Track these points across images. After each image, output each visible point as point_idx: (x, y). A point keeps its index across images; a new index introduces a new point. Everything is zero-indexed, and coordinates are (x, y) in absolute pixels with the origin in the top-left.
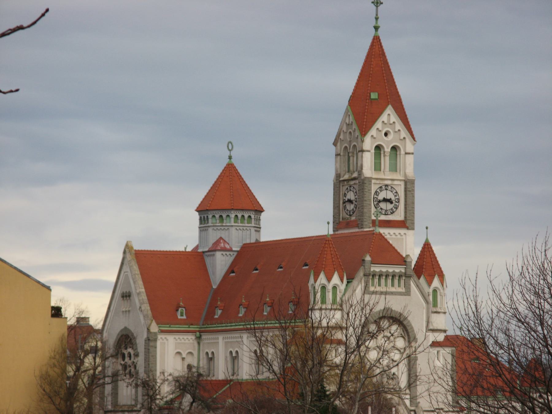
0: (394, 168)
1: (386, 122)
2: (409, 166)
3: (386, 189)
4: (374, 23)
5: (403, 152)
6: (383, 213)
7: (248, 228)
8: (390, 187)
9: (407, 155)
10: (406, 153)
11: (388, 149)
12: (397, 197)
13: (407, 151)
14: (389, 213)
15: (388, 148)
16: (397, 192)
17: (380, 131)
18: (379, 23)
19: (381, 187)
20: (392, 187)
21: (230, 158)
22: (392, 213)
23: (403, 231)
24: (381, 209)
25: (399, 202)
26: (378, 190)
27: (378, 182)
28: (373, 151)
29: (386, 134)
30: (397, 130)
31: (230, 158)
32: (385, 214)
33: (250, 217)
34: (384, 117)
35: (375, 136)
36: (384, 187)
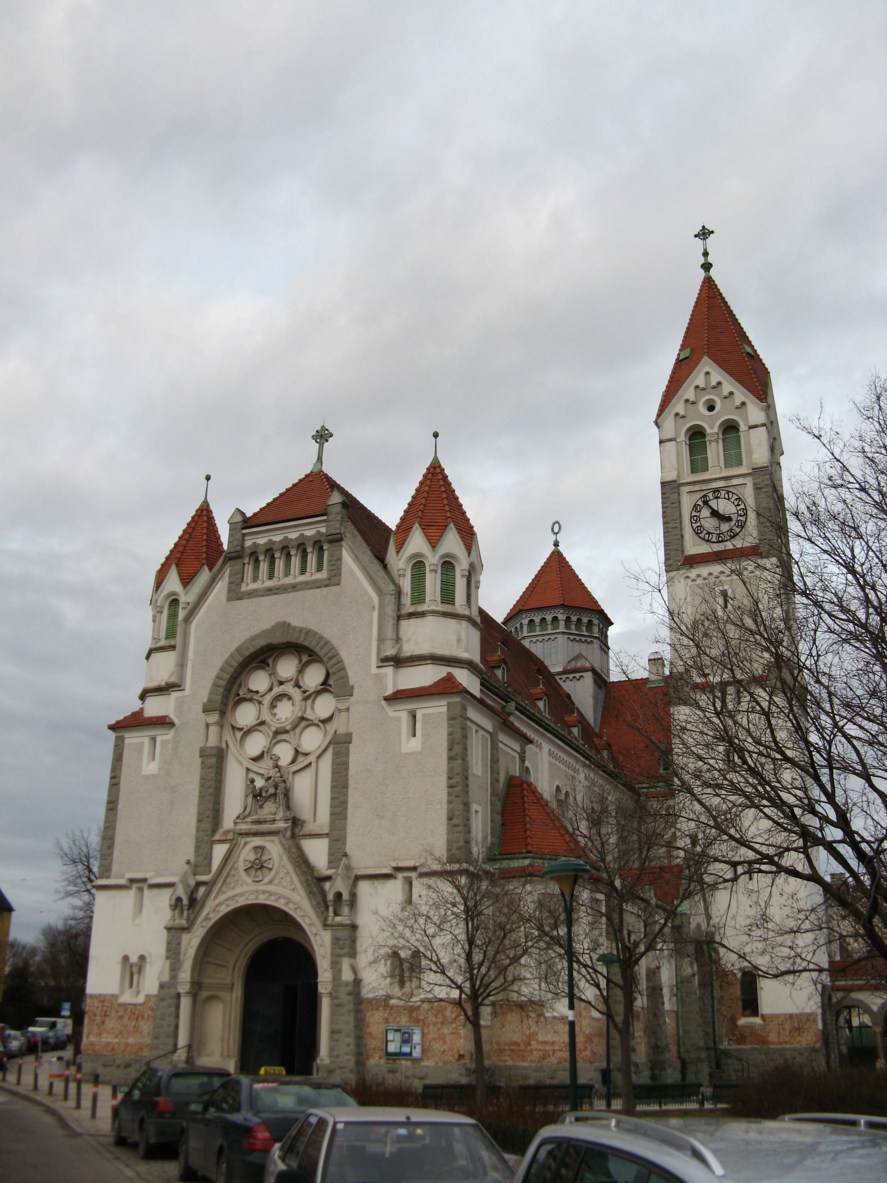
0: (733, 457)
4: (702, 260)
5: (743, 427)
7: (553, 637)
8: (723, 493)
9: (751, 430)
10: (751, 427)
11: (712, 430)
12: (742, 506)
13: (752, 423)
15: (712, 427)
16: (739, 499)
17: (693, 403)
18: (710, 259)
19: (705, 496)
20: (728, 492)
21: (556, 544)
24: (709, 533)
25: (746, 514)
27: (697, 488)
28: (682, 438)
29: (711, 408)
31: (556, 544)
32: (719, 542)
33: (555, 619)
35: (682, 413)
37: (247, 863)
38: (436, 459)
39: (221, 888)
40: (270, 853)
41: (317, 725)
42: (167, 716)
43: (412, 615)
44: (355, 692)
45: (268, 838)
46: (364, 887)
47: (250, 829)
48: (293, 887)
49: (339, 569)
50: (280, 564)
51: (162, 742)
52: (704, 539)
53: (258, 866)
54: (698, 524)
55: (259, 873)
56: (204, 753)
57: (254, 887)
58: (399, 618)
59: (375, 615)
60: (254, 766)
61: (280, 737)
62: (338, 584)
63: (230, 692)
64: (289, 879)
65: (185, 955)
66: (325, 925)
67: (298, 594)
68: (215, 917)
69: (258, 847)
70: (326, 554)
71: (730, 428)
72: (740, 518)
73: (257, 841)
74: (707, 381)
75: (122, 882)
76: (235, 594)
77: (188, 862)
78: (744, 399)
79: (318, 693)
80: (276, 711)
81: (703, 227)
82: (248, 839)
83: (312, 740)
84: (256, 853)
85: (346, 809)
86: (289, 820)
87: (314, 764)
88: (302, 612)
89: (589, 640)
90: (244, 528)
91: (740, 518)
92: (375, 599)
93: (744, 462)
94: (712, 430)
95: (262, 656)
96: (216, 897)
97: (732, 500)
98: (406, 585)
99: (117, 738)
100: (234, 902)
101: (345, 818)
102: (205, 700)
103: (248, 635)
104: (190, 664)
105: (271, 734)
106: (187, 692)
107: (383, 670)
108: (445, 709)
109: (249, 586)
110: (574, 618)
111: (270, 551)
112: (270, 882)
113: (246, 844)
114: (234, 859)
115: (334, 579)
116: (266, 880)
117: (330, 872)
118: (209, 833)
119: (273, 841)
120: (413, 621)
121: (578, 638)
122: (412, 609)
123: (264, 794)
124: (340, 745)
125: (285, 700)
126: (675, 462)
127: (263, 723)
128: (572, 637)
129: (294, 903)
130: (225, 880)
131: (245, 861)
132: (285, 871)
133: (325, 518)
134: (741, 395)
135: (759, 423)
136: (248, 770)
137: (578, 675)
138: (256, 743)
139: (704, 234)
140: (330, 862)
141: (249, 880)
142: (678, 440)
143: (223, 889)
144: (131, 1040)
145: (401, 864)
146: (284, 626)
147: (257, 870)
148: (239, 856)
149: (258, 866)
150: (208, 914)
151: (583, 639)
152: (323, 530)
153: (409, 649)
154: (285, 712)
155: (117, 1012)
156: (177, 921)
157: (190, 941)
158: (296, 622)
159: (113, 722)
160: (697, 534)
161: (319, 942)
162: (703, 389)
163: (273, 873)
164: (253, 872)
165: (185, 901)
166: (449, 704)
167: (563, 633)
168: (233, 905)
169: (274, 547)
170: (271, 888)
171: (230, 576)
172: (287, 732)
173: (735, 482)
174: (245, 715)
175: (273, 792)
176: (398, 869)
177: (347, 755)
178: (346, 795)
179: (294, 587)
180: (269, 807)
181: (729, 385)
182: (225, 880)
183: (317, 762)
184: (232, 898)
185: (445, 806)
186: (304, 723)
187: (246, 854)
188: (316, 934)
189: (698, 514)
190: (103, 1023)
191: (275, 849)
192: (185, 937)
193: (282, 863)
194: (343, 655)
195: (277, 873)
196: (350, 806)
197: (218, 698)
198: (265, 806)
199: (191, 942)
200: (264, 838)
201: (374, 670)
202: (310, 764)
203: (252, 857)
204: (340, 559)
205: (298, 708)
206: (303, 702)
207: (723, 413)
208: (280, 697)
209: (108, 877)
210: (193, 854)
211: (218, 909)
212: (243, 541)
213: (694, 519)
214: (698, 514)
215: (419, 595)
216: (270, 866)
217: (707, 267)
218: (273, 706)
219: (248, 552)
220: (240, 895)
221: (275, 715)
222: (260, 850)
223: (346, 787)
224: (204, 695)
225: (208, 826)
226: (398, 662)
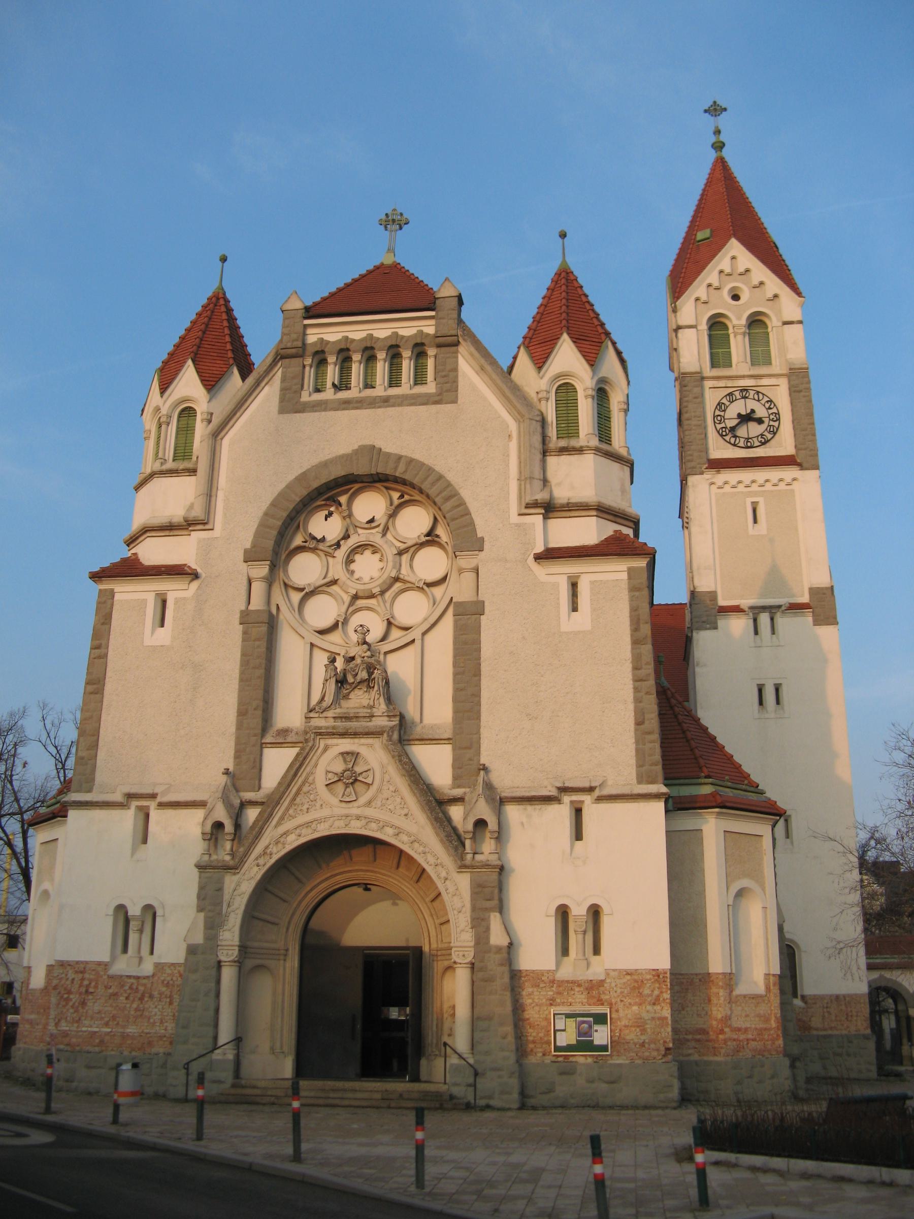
1: (728, 270)
2: (790, 345)
3: (745, 398)
4: (713, 139)
5: (773, 323)
8: (752, 393)
10: (785, 323)
12: (775, 410)
14: (757, 444)
15: (739, 318)
16: (771, 401)
17: (717, 289)
18: (722, 138)
20: (758, 393)
22: (763, 444)
23: (789, 473)
25: (778, 420)
26: (724, 401)
27: (722, 383)
28: (704, 326)
29: (736, 297)
30: (756, 283)
34: (722, 261)
35: (704, 298)
36: (737, 393)
37: (330, 775)
39: (287, 809)
40: (366, 762)
41: (421, 589)
42: (185, 565)
43: (563, 451)
44: (487, 546)
45: (363, 741)
46: (512, 812)
47: (334, 728)
48: (406, 811)
49: (455, 381)
51: (177, 601)
52: (730, 443)
53: (350, 779)
55: (350, 789)
56: (246, 618)
57: (343, 810)
58: (545, 453)
59: (513, 445)
60: (317, 640)
61: (360, 603)
62: (455, 401)
63: (281, 539)
64: (398, 800)
65: (229, 906)
66: (463, 867)
68: (278, 853)
69: (348, 753)
70: (430, 363)
71: (756, 322)
72: (772, 423)
73: (346, 745)
74: (733, 267)
75: (118, 797)
76: (290, 403)
77: (227, 772)
79: (422, 545)
80: (353, 566)
81: (715, 102)
82: (330, 742)
83: (411, 608)
84: (345, 761)
85: (479, 704)
86: (394, 716)
87: (418, 642)
90: (305, 318)
91: (772, 423)
92: (513, 426)
94: (737, 320)
95: (331, 489)
96: (279, 824)
97: (763, 402)
100: (309, 831)
101: (478, 718)
102: (248, 545)
103: (315, 460)
104: (221, 495)
105: (347, 599)
106: (217, 532)
108: (625, 576)
111: (344, 354)
112: (369, 803)
113: (326, 748)
114: (308, 769)
115: (448, 392)
116: (363, 800)
117: (458, 792)
118: (259, 731)
119: (371, 746)
120: (565, 459)
122: (563, 443)
123: (350, 679)
124: (468, 617)
125: (368, 553)
126: (696, 353)
127: (334, 582)
129: (409, 835)
130: (294, 799)
131: (328, 772)
132: (392, 789)
133: (432, 313)
135: (795, 319)
136: (312, 645)
138: (322, 611)
139: (715, 110)
140: (456, 778)
141: (334, 801)
142: (699, 328)
143: (291, 812)
144: (131, 1030)
146: (372, 451)
147: (347, 786)
148: (316, 766)
149: (350, 779)
150: (267, 847)
152: (431, 330)
153: (562, 494)
154: (368, 568)
155: (107, 987)
156: (214, 857)
157: (238, 884)
158: (389, 447)
159: (97, 569)
161: (451, 889)
162: (729, 275)
163: (373, 789)
164: (340, 787)
165: (229, 827)
166: (630, 571)
168: (308, 835)
169: (352, 347)
170: (369, 812)
171: (283, 380)
172: (372, 596)
173: (765, 382)
174: (305, 569)
175: (359, 674)
176: (564, 790)
177: (478, 630)
178: (478, 685)
180: (359, 699)
182: (294, 799)
183: (422, 640)
184: (308, 824)
185: (631, 707)
186: (398, 586)
187: (328, 759)
188: (446, 879)
189: (722, 414)
190: (83, 1003)
191: (375, 756)
192: (230, 881)
193: (387, 778)
194: (466, 494)
195: (380, 790)
196: (484, 701)
197: (270, 544)
198: (352, 696)
199: (241, 887)
200: (356, 740)
201: (514, 518)
202: (413, 641)
203: (339, 767)
204: (455, 369)
205: (390, 564)
206: (398, 557)
207: (750, 303)
208: (360, 548)
209: (90, 791)
210: (232, 760)
211: (282, 840)
212: (305, 334)
213: (719, 419)
214: (722, 414)
215: (568, 425)
216: (369, 781)
217: (719, 146)
218: (349, 561)
219: (310, 350)
220: (319, 821)
222: (351, 756)
223: (477, 673)
224: (246, 540)
225: (256, 721)
226: (549, 509)
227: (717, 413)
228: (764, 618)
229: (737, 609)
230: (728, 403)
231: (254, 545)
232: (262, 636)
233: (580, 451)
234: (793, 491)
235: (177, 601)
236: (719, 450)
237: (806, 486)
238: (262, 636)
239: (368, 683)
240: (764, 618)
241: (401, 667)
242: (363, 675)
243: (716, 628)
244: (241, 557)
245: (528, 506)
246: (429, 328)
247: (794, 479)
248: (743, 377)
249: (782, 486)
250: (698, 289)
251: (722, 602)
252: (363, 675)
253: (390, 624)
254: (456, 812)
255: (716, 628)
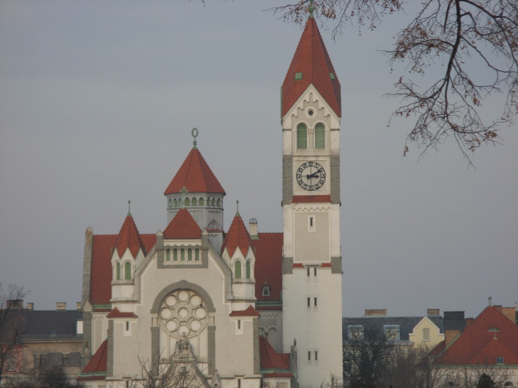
0: (320, 144)
1: (308, 100)
3: (311, 166)
5: (327, 129)
6: (308, 189)
7: (200, 210)
8: (314, 164)
9: (332, 132)
10: (332, 130)
11: (311, 127)
13: (332, 128)
14: (314, 189)
15: (311, 126)
17: (302, 110)
19: (305, 164)
20: (317, 164)
21: (195, 143)
22: (317, 189)
23: (326, 205)
24: (305, 185)
25: (325, 177)
26: (302, 167)
27: (301, 159)
28: (295, 129)
29: (311, 113)
30: (320, 108)
31: (195, 143)
32: (310, 190)
33: (201, 199)
34: (306, 96)
35: (296, 115)
36: (308, 164)
38: (238, 213)
43: (237, 283)
44: (216, 311)
46: (223, 382)
49: (207, 261)
50: (179, 255)
54: (300, 179)
58: (232, 283)
59: (224, 282)
61: (182, 324)
63: (159, 306)
67: (190, 270)
70: (200, 254)
71: (320, 126)
72: (322, 179)
73: (182, 365)
74: (311, 98)
76: (160, 265)
78: (330, 113)
79: (198, 308)
80: (180, 313)
83: (196, 326)
88: (192, 276)
89: (218, 210)
91: (322, 179)
92: (223, 276)
93: (326, 147)
94: (311, 127)
98: (233, 270)
99: (109, 321)
102: (151, 308)
106: (142, 304)
107: (227, 304)
108: (252, 320)
109: (166, 263)
110: (211, 199)
115: (205, 265)
117: (210, 376)
120: (237, 285)
121: (213, 210)
122: (237, 281)
124: (212, 330)
125: (183, 309)
126: (290, 143)
128: (210, 210)
134: (328, 110)
137: (214, 234)
138: (172, 326)
142: (293, 130)
145: (237, 375)
151: (215, 210)
153: (237, 295)
154: (184, 314)
158: (190, 281)
160: (300, 184)
162: (308, 102)
166: (254, 319)
167: (207, 208)
171: (158, 257)
172: (185, 322)
173: (320, 159)
174: (166, 314)
175: (183, 345)
176: (236, 376)
177: (214, 334)
179: (188, 266)
181: (322, 103)
185: (253, 355)
186: (192, 319)
189: (300, 173)
194: (211, 296)
201: (224, 303)
204: (207, 258)
207: (316, 118)
209: (112, 376)
213: (299, 176)
214: (300, 173)
215: (238, 275)
218: (179, 311)
219: (166, 248)
221: (179, 315)
222: (185, 368)
226: (233, 301)
227: (298, 173)
228: (312, 270)
229: (300, 266)
230: (303, 169)
231: (153, 309)
232: (156, 332)
233: (241, 283)
234: (328, 213)
235: (132, 324)
236: (298, 191)
237: (333, 211)
238: (156, 332)
239: (187, 348)
240: (312, 270)
241: (193, 342)
242: (185, 346)
243: (292, 273)
244: (149, 312)
245: (227, 300)
246: (200, 244)
247: (329, 208)
248: (311, 156)
249: (323, 211)
250: (294, 111)
251: (295, 262)
252: (185, 346)
253: (190, 330)
254: (210, 381)
255: (292, 273)
